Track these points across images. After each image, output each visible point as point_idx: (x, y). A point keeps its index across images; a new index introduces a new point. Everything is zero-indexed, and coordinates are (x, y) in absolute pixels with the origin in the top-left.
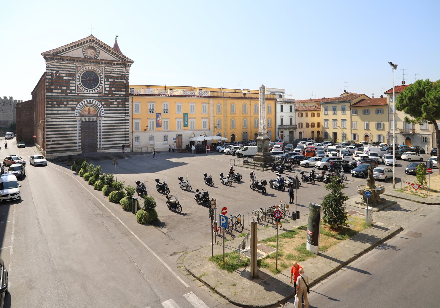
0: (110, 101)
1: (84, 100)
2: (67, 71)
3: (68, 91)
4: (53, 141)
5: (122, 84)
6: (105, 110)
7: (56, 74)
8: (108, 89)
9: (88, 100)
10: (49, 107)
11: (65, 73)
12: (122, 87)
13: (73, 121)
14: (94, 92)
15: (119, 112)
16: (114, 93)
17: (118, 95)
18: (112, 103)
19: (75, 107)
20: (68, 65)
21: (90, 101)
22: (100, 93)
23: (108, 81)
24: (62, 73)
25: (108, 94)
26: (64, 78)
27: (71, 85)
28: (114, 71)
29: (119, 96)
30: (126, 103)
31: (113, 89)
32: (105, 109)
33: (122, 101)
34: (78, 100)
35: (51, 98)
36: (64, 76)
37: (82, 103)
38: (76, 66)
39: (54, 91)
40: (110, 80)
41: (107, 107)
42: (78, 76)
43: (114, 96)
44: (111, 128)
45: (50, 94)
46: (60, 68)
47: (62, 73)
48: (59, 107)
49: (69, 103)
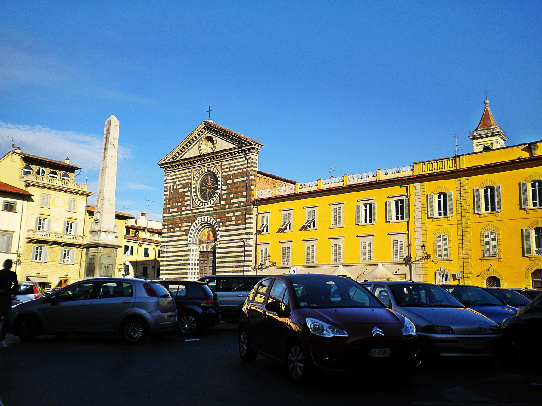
0: (227, 215)
1: (198, 218)
2: (182, 180)
3: (183, 208)
5: (242, 184)
6: (221, 231)
8: (225, 197)
9: (202, 218)
10: (165, 233)
11: (182, 184)
12: (242, 189)
13: (185, 251)
14: (210, 205)
15: (238, 232)
16: (232, 201)
17: (237, 205)
19: (189, 230)
22: (216, 204)
23: (226, 184)
24: (179, 185)
25: (224, 205)
26: (181, 191)
27: (186, 198)
28: (232, 167)
29: (238, 207)
30: (247, 216)
31: (232, 196)
32: (220, 229)
33: (242, 215)
34: (191, 219)
35: (168, 220)
36: (180, 189)
37: (196, 223)
38: (192, 171)
39: (171, 210)
40: (228, 182)
42: (194, 184)
43: (233, 207)
44: (227, 260)
46: (177, 178)
47: (179, 185)
48: (174, 232)
49: (184, 225)
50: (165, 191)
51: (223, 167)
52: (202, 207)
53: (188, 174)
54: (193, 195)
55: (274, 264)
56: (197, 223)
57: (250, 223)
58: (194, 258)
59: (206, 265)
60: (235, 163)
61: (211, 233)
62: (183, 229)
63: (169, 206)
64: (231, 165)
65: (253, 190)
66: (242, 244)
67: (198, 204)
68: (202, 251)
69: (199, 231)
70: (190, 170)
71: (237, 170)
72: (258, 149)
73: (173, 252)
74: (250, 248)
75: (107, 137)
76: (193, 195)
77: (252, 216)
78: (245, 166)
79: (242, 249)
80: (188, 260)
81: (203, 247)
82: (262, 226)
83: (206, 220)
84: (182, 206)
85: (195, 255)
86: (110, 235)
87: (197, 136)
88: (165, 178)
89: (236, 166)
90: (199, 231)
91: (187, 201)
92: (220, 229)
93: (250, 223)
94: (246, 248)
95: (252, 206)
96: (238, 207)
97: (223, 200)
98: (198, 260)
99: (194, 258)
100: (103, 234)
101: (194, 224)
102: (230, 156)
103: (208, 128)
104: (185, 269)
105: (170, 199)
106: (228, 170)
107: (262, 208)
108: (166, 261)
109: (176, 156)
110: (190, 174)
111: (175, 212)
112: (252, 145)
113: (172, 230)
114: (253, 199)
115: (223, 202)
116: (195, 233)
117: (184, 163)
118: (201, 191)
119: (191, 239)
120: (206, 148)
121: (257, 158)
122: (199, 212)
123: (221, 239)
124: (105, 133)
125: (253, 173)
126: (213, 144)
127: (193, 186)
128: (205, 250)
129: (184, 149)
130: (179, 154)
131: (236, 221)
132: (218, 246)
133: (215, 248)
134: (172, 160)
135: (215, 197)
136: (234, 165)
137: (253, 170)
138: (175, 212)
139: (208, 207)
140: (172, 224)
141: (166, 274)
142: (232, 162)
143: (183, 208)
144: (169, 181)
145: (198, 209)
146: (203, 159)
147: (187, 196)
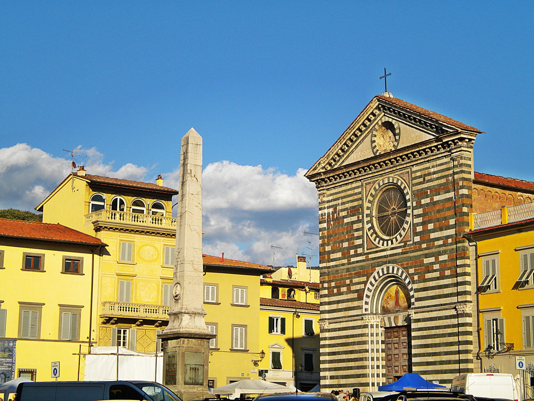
0: (426, 261)
2: (348, 202)
4: (332, 377)
7: (333, 213)
8: (419, 229)
9: (385, 267)
10: (325, 296)
14: (395, 244)
16: (433, 236)
17: (441, 242)
18: (429, 269)
20: (349, 187)
21: (388, 268)
23: (419, 205)
25: (420, 243)
26: (346, 220)
27: (356, 234)
28: (429, 174)
29: (444, 245)
30: (459, 262)
31: (431, 226)
32: (415, 286)
33: (451, 259)
36: (344, 217)
37: (374, 278)
38: (362, 184)
39: (333, 256)
40: (423, 202)
41: (419, 281)
42: (368, 208)
44: (429, 341)
45: (324, 265)
46: (338, 199)
48: (340, 293)
49: (355, 280)
50: (320, 223)
51: (413, 176)
52: (382, 248)
53: (356, 191)
54: (369, 225)
55: (511, 347)
56: (377, 278)
57: (465, 274)
58: (375, 338)
59: (396, 352)
60: (433, 167)
61: (401, 294)
62: (353, 288)
63: (328, 248)
64: (426, 172)
65: (467, 214)
66: (453, 312)
67: (376, 243)
68: (388, 326)
69: (381, 291)
70: (359, 184)
71: (438, 179)
72: (470, 140)
73: (340, 329)
74: (468, 320)
75: (184, 165)
76: (367, 226)
77: (467, 262)
78: (451, 172)
79: (455, 321)
80: (365, 343)
81: (389, 319)
82: (486, 279)
83: (391, 271)
84: (349, 248)
85: (377, 335)
86: (197, 318)
87: (368, 123)
88: (319, 201)
89: (434, 173)
90: (381, 291)
91: (358, 238)
92: (415, 286)
93: (465, 274)
94: (461, 320)
95: (466, 244)
96: (444, 245)
97: (416, 234)
98: (383, 342)
99: (375, 338)
100: (186, 318)
101: (371, 279)
102: (424, 155)
103: (383, 107)
104: (361, 359)
105: (329, 236)
106: (421, 180)
107: (485, 246)
108: (330, 346)
109: (335, 160)
110: (360, 190)
111: (339, 259)
112: (457, 133)
113: (335, 291)
114: (467, 230)
115: (417, 239)
116: (374, 295)
117: (348, 172)
118: (380, 219)
119: (368, 307)
120: (384, 142)
121: (471, 155)
122: (379, 258)
123: (417, 304)
124: (182, 157)
125: (465, 183)
126: (395, 135)
127: (367, 212)
128: (394, 325)
129: (348, 146)
130: (339, 156)
131: (441, 270)
132: (414, 317)
133: (408, 319)
134: (329, 168)
135: (404, 229)
136: (432, 170)
137: (464, 179)
138: (339, 259)
139: (392, 249)
140: (333, 282)
141: (330, 369)
142: (428, 165)
143: (352, 252)
144: (326, 205)
145: (377, 252)
146: (379, 163)
147: (357, 230)
